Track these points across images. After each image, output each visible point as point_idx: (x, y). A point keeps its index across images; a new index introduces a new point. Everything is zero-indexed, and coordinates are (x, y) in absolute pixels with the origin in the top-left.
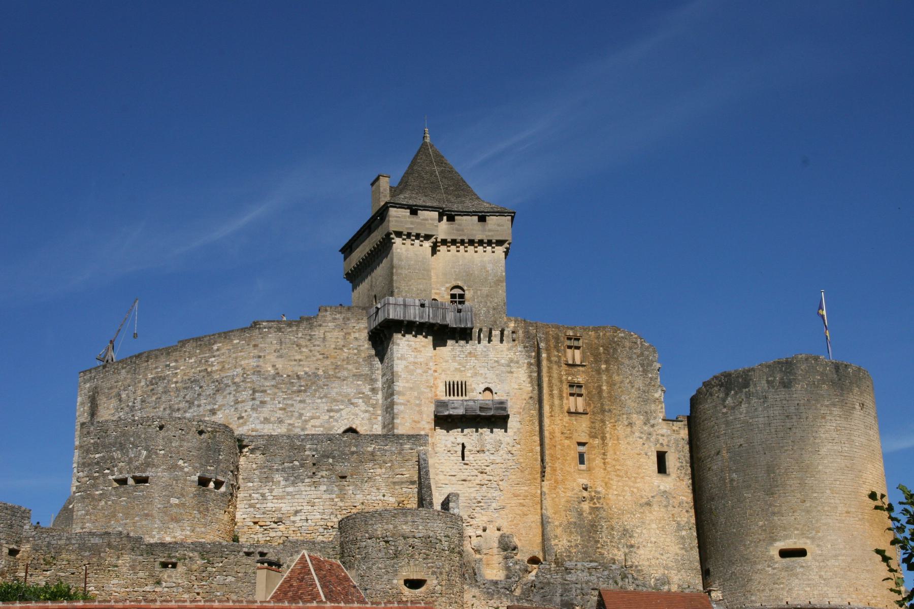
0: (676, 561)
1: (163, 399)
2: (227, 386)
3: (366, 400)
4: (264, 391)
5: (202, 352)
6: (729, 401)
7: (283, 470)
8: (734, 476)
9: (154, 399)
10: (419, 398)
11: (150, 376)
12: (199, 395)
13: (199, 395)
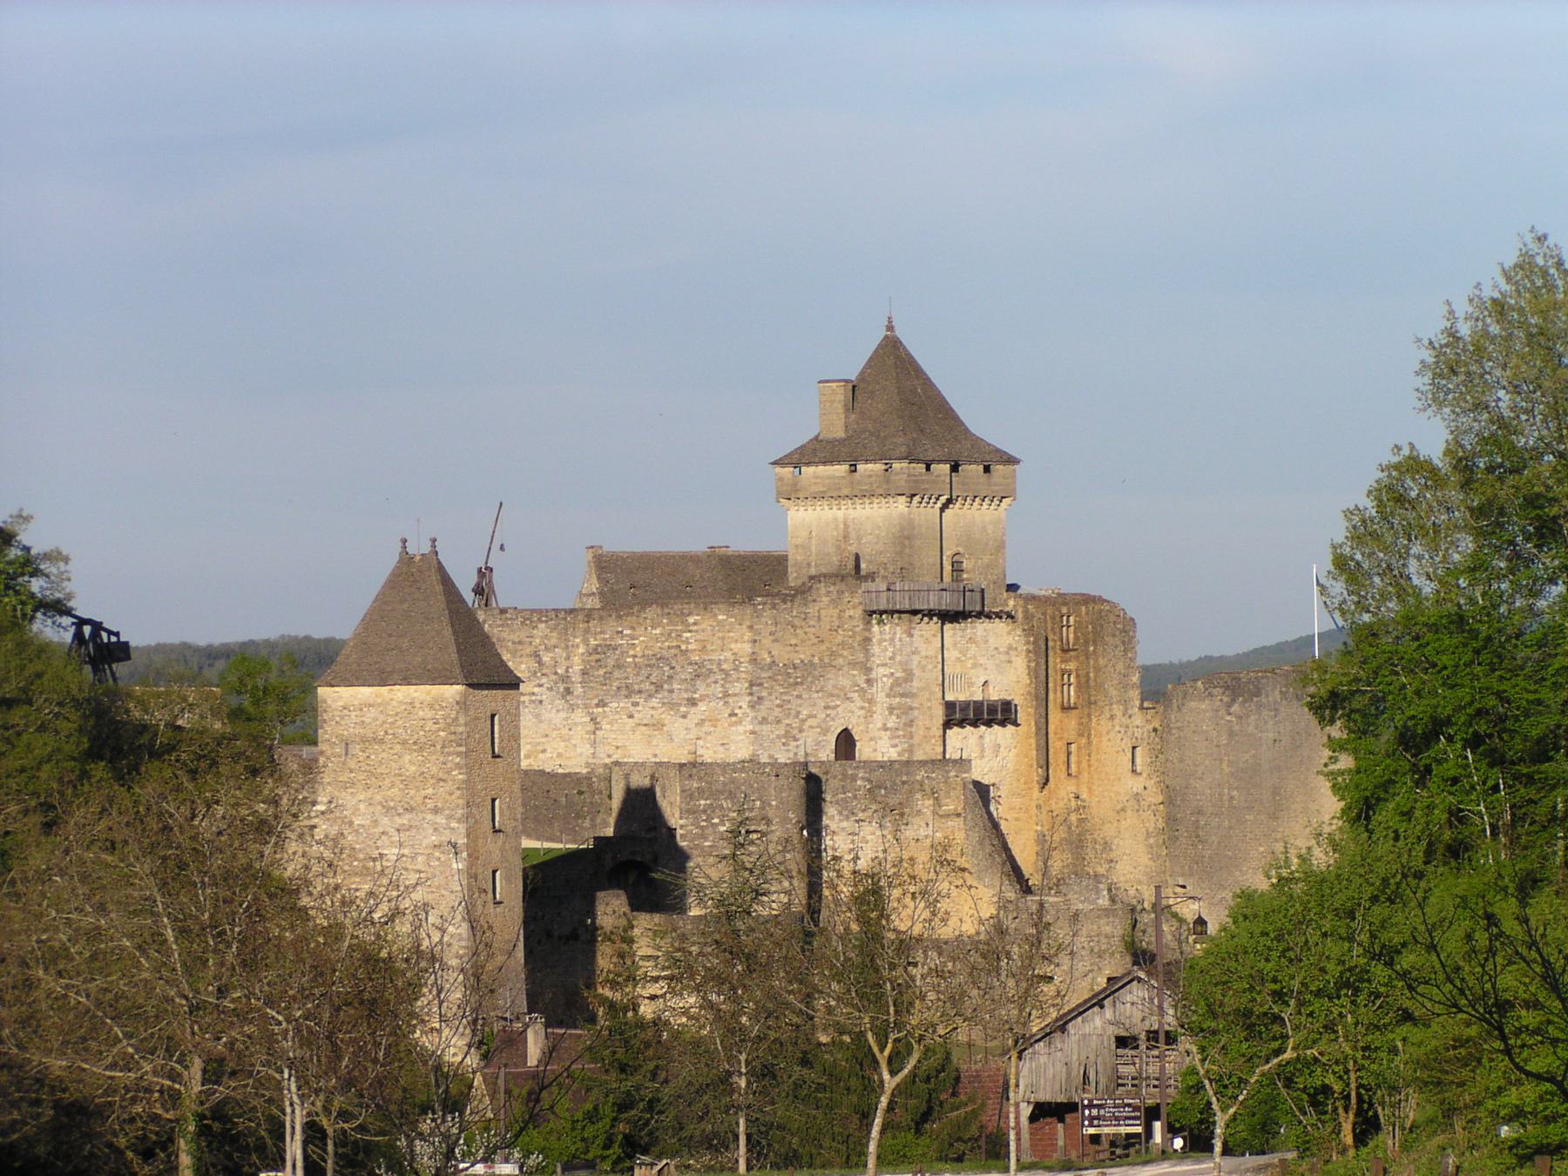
0: (1146, 874)
1: (616, 674)
2: (710, 671)
3: (862, 691)
4: (761, 684)
5: (671, 623)
6: (1235, 708)
7: (837, 803)
8: (1235, 793)
9: (601, 672)
10: (929, 700)
11: (593, 642)
12: (670, 677)
13: (670, 677)
